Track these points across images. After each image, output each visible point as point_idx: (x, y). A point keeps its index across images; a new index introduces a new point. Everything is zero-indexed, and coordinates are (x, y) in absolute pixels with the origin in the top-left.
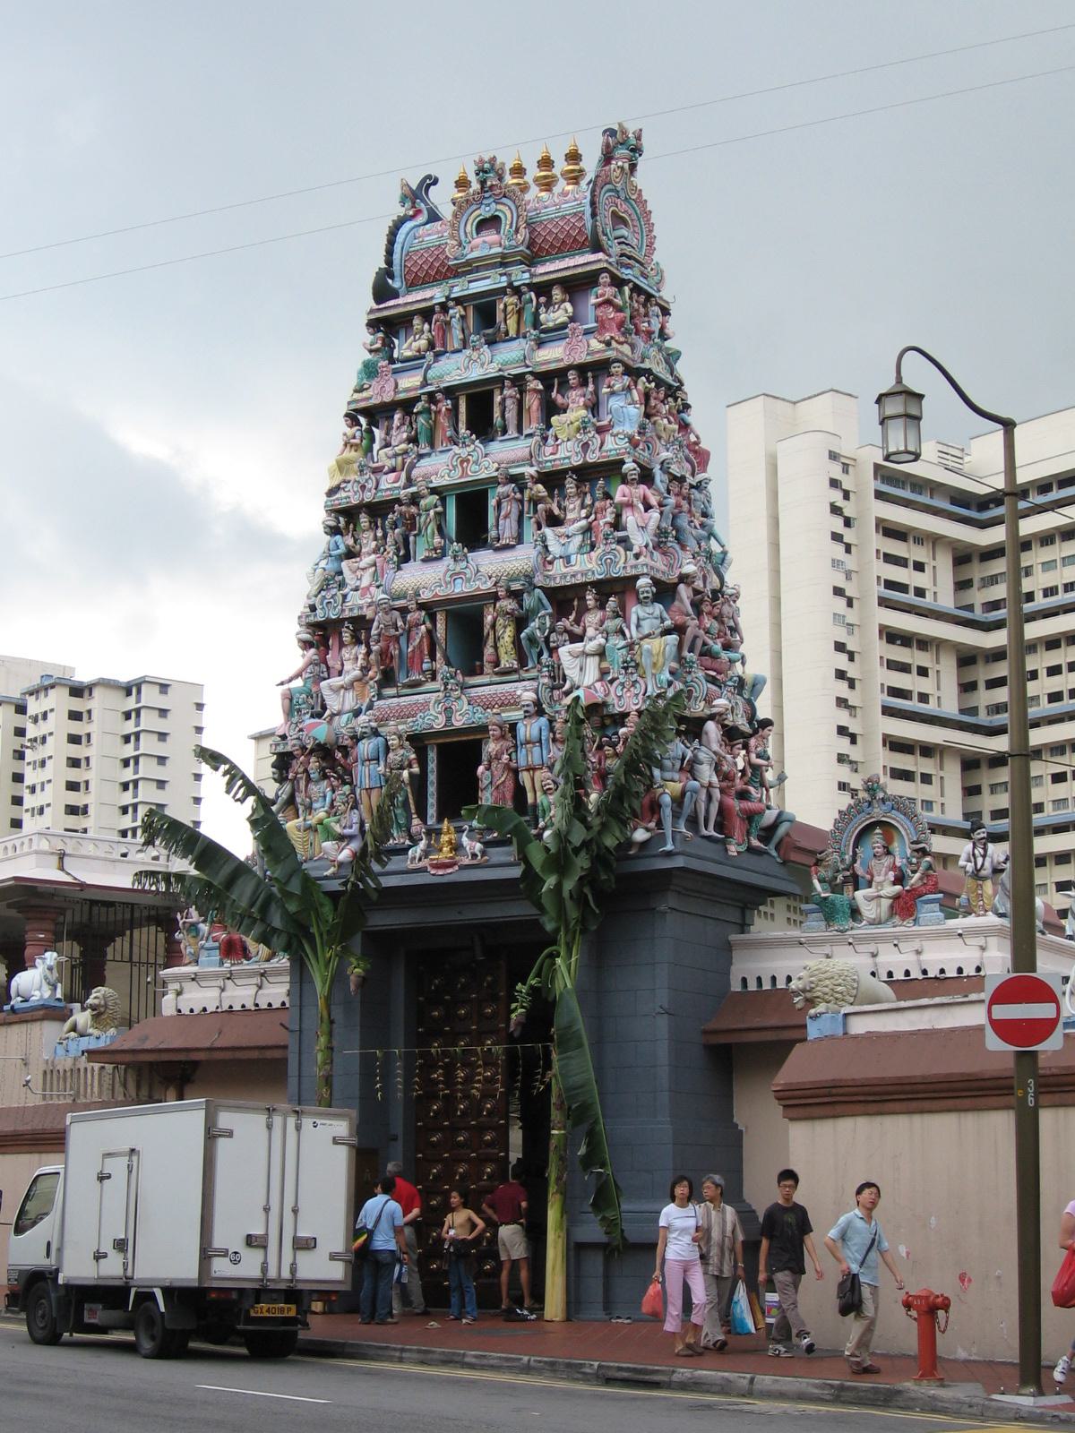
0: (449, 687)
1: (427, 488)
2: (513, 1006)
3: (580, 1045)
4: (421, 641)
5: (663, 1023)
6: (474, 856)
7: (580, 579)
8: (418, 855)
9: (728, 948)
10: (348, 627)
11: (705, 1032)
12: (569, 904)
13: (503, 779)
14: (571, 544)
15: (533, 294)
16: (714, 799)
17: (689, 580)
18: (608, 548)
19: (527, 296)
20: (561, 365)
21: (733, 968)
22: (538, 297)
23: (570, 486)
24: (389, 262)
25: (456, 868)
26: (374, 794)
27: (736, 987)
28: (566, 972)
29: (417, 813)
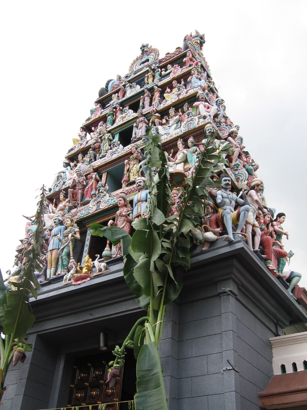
0: (101, 191)
1: (106, 131)
2: (111, 363)
3: (158, 386)
4: (92, 184)
5: (231, 379)
6: (100, 270)
7: (174, 136)
8: (68, 277)
9: (269, 346)
10: (63, 192)
11: (262, 397)
12: (155, 276)
13: (123, 226)
14: (171, 129)
15: (159, 70)
16: (257, 234)
17: (234, 134)
18: (190, 119)
19: (157, 70)
20: (170, 79)
21: (274, 359)
22: (161, 69)
23: (172, 111)
24: (107, 87)
25: (89, 279)
26: (54, 252)
27: (277, 372)
28: (153, 333)
29: (73, 256)
